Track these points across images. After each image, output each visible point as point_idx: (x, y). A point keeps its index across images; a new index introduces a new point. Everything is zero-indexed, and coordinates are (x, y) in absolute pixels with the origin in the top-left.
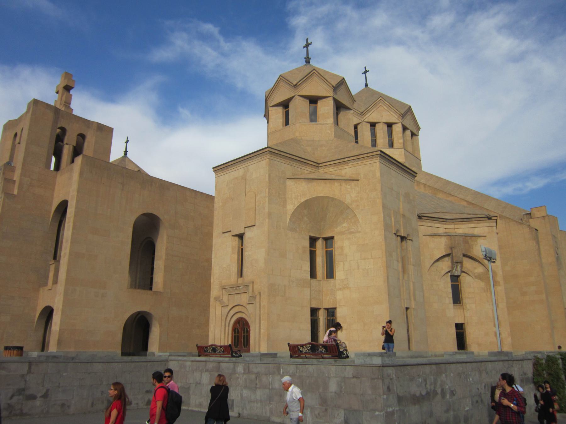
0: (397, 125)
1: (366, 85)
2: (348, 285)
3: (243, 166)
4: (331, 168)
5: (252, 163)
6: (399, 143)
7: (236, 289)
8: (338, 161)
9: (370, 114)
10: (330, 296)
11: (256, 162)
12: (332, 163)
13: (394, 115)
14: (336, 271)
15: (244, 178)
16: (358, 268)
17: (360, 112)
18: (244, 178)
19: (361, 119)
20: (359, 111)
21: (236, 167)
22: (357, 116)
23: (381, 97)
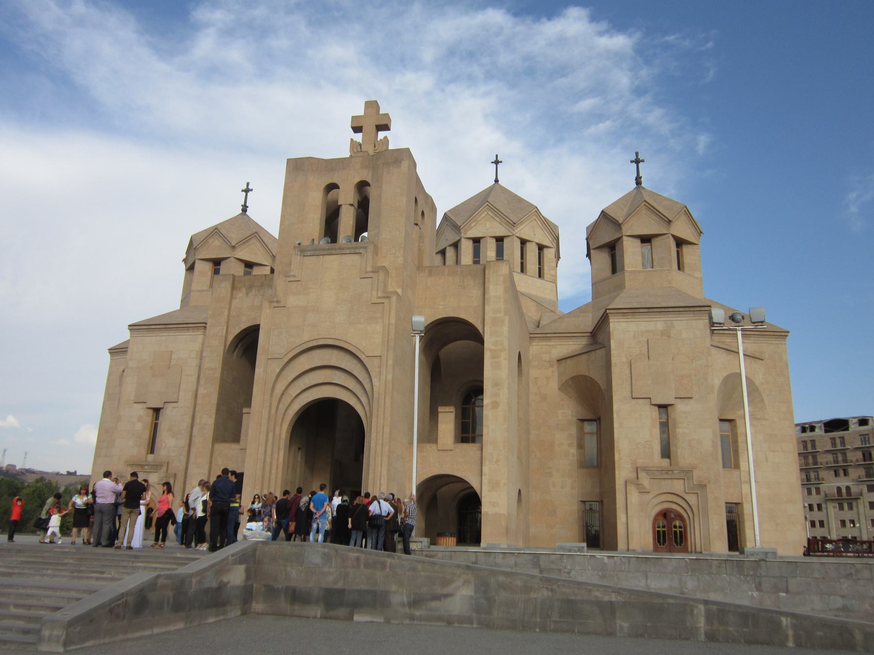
0: (550, 250)
1: (497, 181)
3: (664, 319)
4: (729, 338)
5: (680, 319)
6: (551, 275)
7: (667, 473)
9: (522, 227)
11: (687, 318)
13: (548, 235)
14: (741, 460)
15: (666, 333)
16: (767, 461)
17: (511, 221)
18: (666, 333)
19: (512, 231)
20: (510, 220)
22: (506, 226)
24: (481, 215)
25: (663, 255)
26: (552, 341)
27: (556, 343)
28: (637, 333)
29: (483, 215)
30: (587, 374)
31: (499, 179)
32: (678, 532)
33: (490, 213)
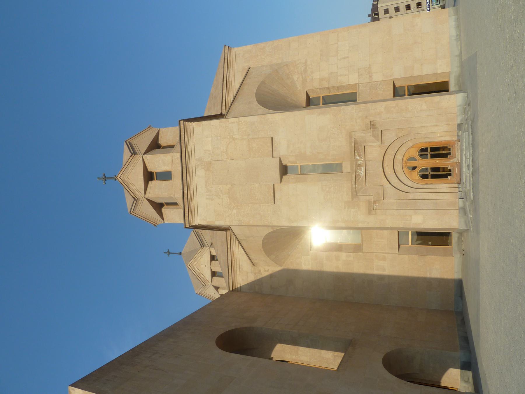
2: (366, 68)
3: (194, 168)
5: (193, 152)
8: (224, 91)
10: (378, 90)
11: (193, 144)
12: (224, 99)
15: (208, 166)
16: (348, 57)
18: (208, 166)
21: (192, 184)
23: (180, 121)
24: (196, 270)
25: (161, 162)
26: (236, 269)
27: (238, 265)
28: (208, 197)
29: (197, 269)
30: (261, 243)
31: (179, 252)
32: (432, 153)
33: (195, 264)
